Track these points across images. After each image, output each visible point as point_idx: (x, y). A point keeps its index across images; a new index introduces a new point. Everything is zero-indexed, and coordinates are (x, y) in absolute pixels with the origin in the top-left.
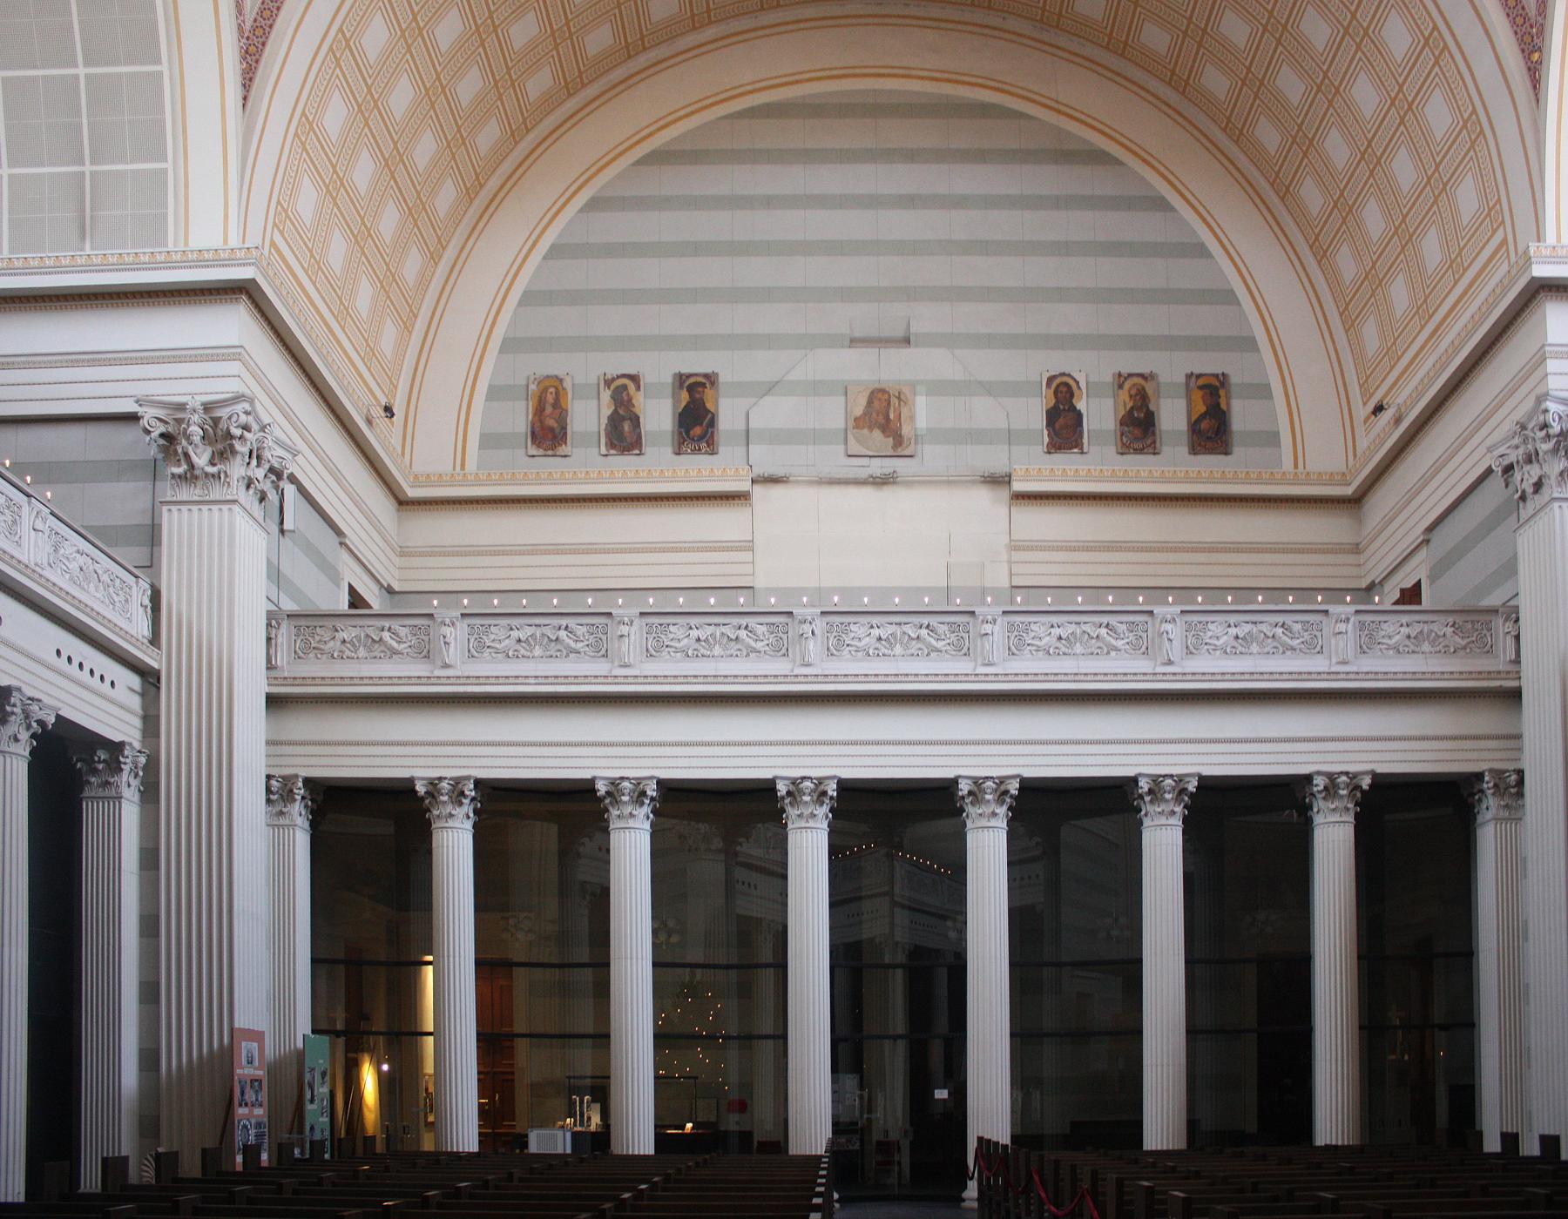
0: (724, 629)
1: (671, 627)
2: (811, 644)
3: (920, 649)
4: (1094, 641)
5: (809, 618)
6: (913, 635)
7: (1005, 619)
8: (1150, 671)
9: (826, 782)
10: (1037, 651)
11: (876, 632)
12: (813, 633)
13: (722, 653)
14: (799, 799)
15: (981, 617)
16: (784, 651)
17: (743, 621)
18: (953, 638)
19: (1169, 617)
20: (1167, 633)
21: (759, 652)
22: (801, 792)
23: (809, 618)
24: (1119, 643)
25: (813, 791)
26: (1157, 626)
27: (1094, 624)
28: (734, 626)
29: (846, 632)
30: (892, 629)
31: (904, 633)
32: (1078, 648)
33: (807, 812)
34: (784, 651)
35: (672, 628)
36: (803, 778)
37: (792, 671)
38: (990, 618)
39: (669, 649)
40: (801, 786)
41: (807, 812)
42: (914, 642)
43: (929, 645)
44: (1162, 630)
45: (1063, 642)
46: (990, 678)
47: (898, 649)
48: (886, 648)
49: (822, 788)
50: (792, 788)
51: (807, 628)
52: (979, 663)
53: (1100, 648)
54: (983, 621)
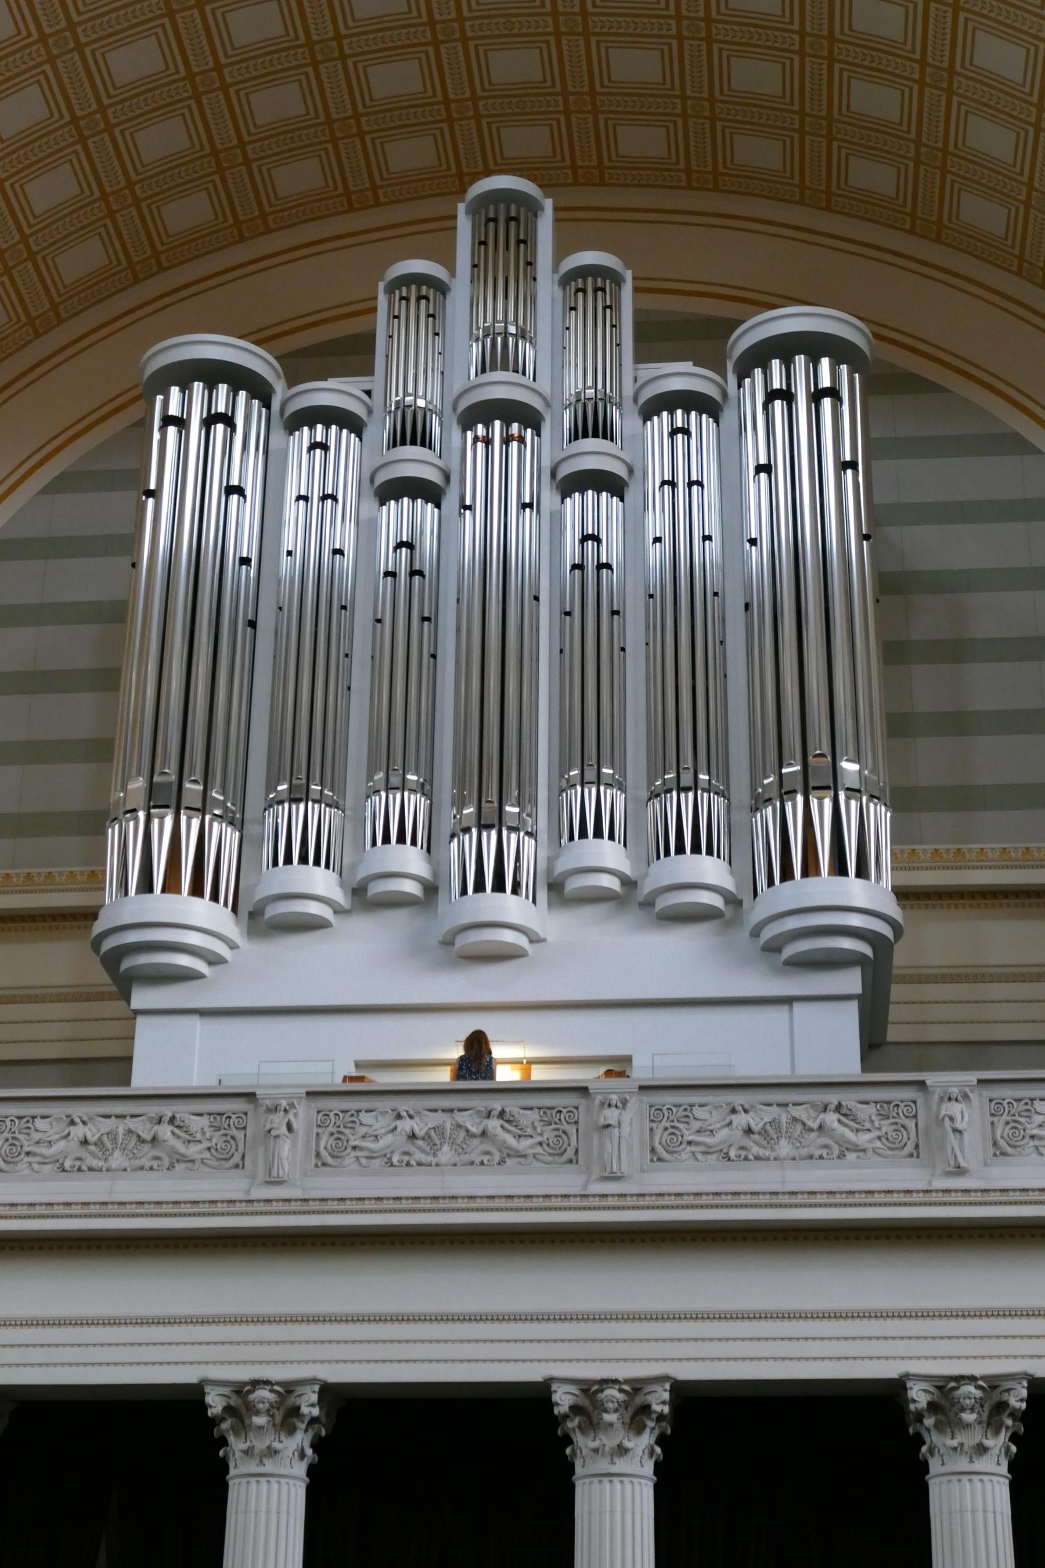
0: (131, 1124)
1: (38, 1121)
2: (285, 1148)
3: (487, 1153)
4: (813, 1135)
5: (284, 1103)
6: (474, 1130)
7: (645, 1099)
8: (922, 1185)
9: (300, 1390)
10: (704, 1153)
11: (406, 1125)
12: (290, 1127)
13: (126, 1164)
14: (247, 1422)
15: (599, 1098)
16: (237, 1158)
17: (167, 1110)
18: (549, 1133)
19: (955, 1091)
20: (951, 1119)
21: (193, 1161)
22: (252, 1409)
23: (284, 1103)
24: (863, 1138)
25: (274, 1406)
26: (934, 1107)
27: (814, 1105)
28: (151, 1119)
29: (352, 1126)
30: (439, 1118)
31: (459, 1126)
32: (785, 1148)
33: (260, 1445)
34: (237, 1158)
35: (39, 1124)
36: (256, 1383)
37: (248, 1192)
38: (614, 1098)
39: (31, 1159)
40: (252, 1397)
41: (260, 1445)
42: (475, 1142)
43: (503, 1146)
44: (943, 1112)
45: (756, 1137)
46: (610, 1202)
47: (446, 1154)
48: (422, 1151)
49: (292, 1400)
50: (234, 1401)
51: (278, 1121)
52: (594, 1176)
53: (826, 1147)
54: (602, 1104)
